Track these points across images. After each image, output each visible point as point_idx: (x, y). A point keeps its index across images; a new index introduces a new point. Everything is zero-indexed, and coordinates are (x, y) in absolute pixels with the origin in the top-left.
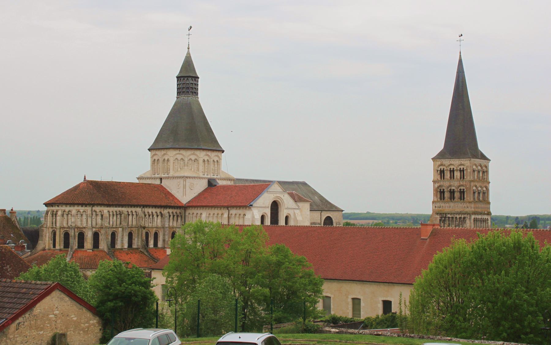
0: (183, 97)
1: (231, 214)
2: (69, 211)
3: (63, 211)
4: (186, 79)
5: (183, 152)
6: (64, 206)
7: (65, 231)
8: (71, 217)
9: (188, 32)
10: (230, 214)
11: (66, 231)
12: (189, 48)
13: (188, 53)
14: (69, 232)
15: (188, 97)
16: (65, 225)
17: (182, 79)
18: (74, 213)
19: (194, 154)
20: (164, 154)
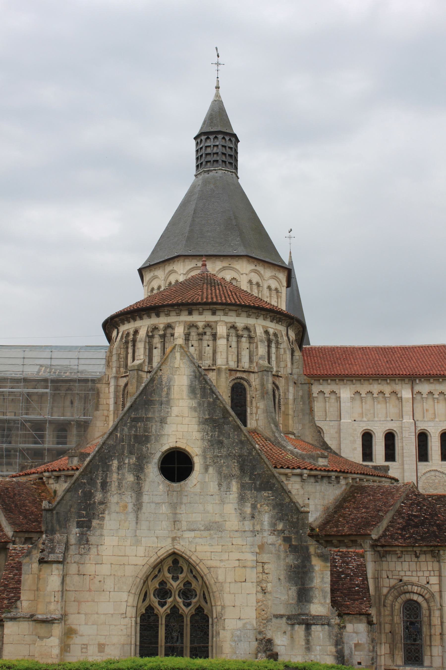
0: (223, 170)
1: (419, 393)
2: (247, 328)
3: (229, 325)
4: (227, 138)
5: (260, 268)
6: (233, 314)
7: (237, 378)
8: (247, 345)
9: (215, 60)
10: (415, 392)
11: (239, 381)
12: (218, 88)
13: (217, 95)
14: (245, 383)
15: (232, 172)
16: (233, 365)
17: (220, 136)
18: (261, 333)
19: (275, 278)
20: (224, 269)
